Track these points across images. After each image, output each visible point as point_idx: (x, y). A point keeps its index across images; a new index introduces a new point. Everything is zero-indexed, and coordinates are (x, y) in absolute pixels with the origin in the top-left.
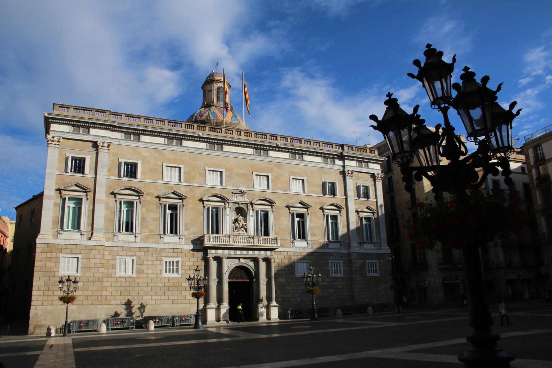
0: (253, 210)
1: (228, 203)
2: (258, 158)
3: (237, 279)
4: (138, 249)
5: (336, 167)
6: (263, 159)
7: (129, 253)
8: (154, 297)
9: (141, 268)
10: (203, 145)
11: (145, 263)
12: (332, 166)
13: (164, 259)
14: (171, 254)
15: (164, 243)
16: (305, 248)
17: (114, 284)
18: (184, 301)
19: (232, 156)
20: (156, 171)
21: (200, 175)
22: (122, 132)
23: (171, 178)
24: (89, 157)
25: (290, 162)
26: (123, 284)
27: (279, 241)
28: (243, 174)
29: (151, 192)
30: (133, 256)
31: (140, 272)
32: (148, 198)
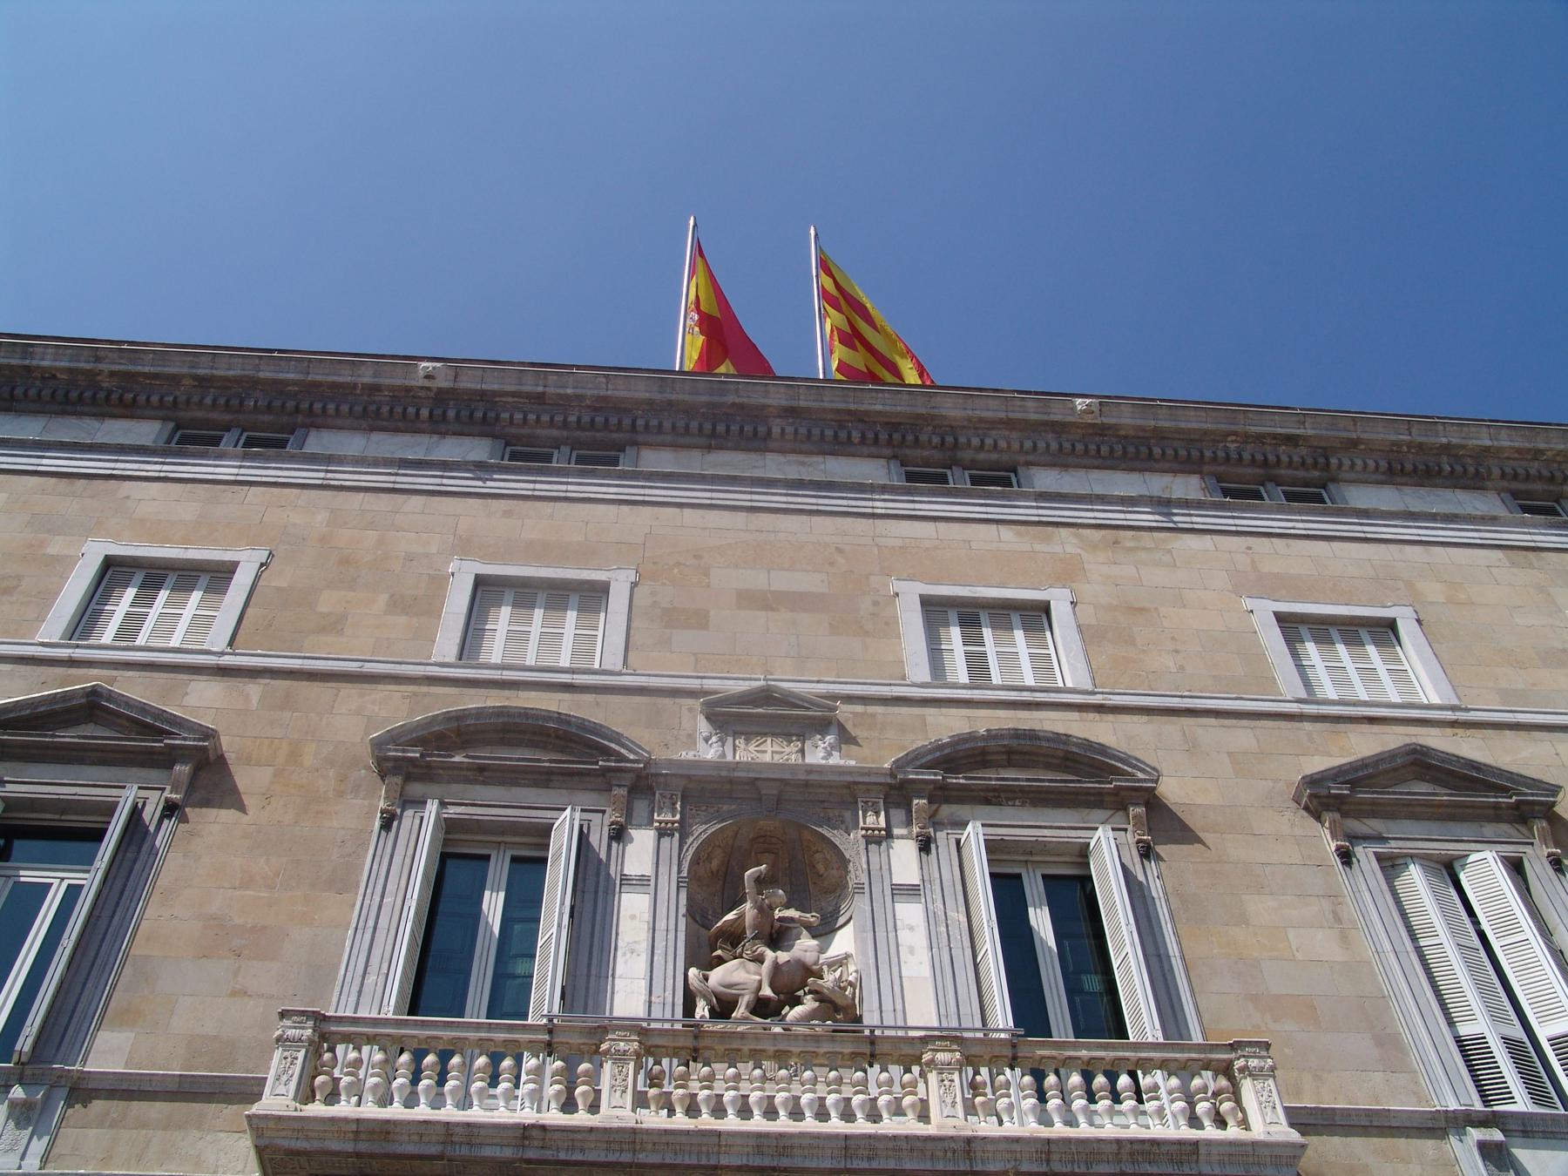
21: (399, 605)
28: (799, 601)
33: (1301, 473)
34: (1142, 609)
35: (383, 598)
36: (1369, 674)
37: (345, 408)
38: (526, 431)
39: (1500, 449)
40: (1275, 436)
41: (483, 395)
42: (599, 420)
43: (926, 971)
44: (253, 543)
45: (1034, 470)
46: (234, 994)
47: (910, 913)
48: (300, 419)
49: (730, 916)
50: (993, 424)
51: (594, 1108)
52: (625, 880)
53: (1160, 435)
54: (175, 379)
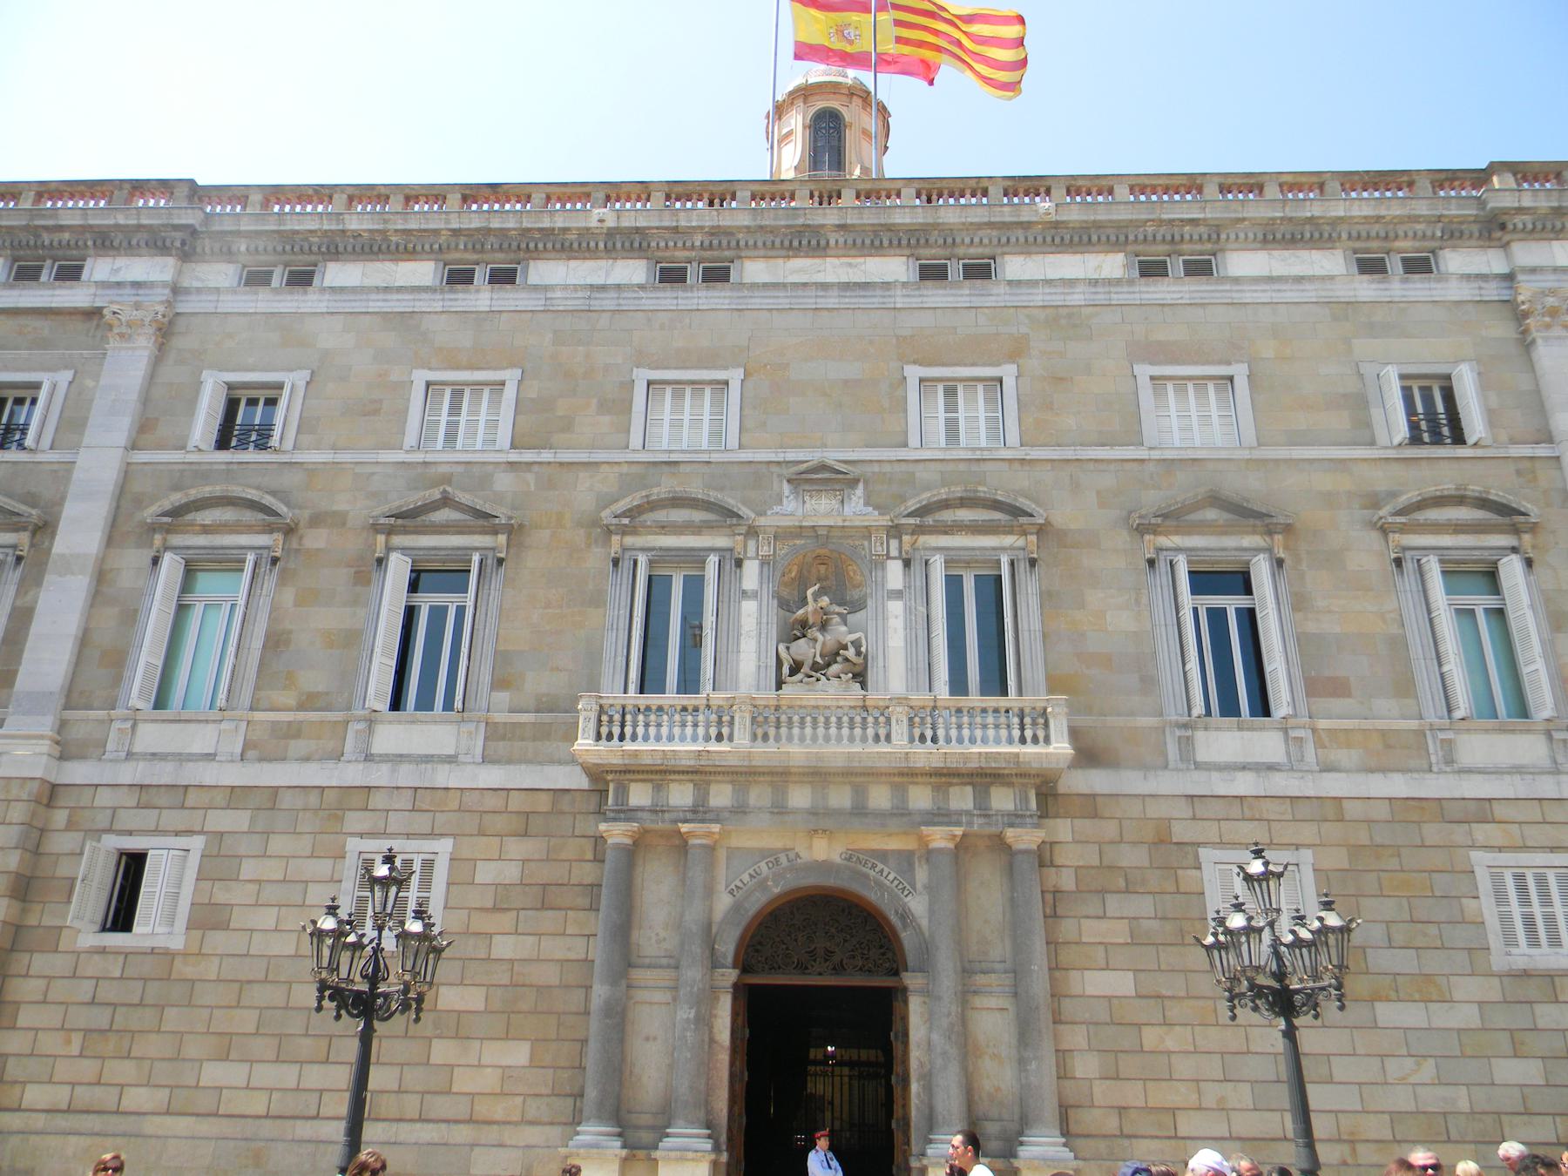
0: (907, 564)
1: (752, 532)
2: (935, 296)
3: (802, 968)
4: (220, 799)
5: (1455, 291)
6: (963, 301)
7: (172, 819)
8: (267, 1074)
9: (221, 896)
10: (633, 271)
11: (248, 869)
12: (1419, 289)
13: (354, 845)
14: (395, 822)
15: (369, 758)
16: (1271, 768)
17: (59, 990)
18: (441, 1106)
19: (784, 303)
20: (376, 412)
21: (604, 407)
22: (228, 255)
23: (451, 437)
24: (68, 375)
25: (1136, 298)
26: (108, 992)
27: (1059, 727)
29: (341, 505)
30: (190, 832)
31: (207, 918)
32: (315, 539)
33: (1198, 247)
34: (1061, 379)
35: (595, 401)
36: (1205, 419)
37: (549, 246)
38: (668, 254)
39: (1352, 217)
40: (1182, 220)
41: (637, 230)
42: (715, 242)
43: (902, 644)
44: (512, 366)
45: (1007, 258)
46: (552, 669)
47: (895, 607)
48: (522, 254)
49: (801, 612)
50: (980, 226)
51: (731, 739)
52: (744, 592)
53: (1098, 225)
54: (436, 232)
